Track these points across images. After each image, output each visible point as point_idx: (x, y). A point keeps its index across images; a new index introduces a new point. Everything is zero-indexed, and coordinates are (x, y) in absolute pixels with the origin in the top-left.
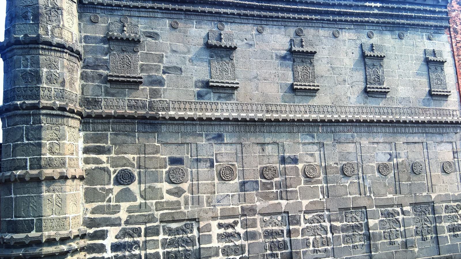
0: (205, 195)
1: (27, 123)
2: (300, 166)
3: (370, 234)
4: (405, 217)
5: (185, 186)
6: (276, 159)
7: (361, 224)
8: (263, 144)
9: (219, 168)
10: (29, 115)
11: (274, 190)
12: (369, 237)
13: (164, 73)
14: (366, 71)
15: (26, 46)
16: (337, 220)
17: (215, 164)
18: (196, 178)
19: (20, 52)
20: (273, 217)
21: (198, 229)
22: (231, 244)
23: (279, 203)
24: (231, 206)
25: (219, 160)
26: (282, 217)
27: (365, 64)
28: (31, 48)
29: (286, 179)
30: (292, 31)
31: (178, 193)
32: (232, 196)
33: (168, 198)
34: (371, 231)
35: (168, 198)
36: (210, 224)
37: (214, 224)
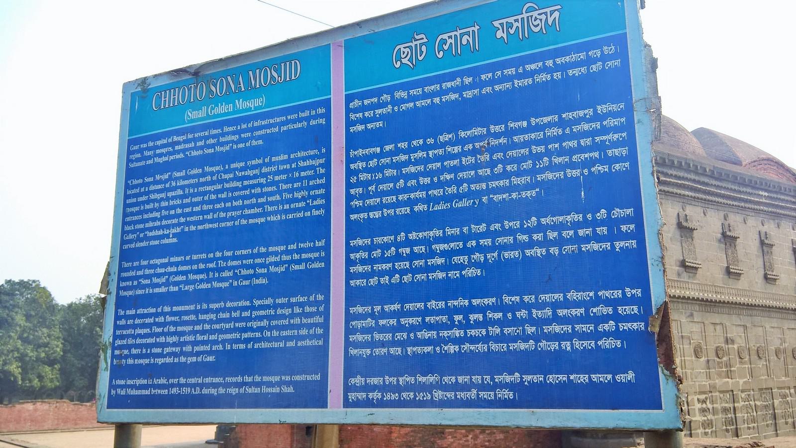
0: (689, 371)
2: (736, 346)
3: (775, 414)
4: (792, 399)
6: (722, 339)
7: (769, 404)
8: (714, 324)
9: (694, 345)
11: (724, 369)
14: (764, 258)
16: (759, 400)
17: (692, 341)
18: (728, 354)
20: (725, 394)
22: (706, 418)
23: (728, 382)
24: (704, 383)
25: (693, 338)
26: (729, 394)
27: (763, 251)
29: (730, 358)
30: (722, 214)
32: (703, 372)
34: (776, 411)
36: (693, 399)
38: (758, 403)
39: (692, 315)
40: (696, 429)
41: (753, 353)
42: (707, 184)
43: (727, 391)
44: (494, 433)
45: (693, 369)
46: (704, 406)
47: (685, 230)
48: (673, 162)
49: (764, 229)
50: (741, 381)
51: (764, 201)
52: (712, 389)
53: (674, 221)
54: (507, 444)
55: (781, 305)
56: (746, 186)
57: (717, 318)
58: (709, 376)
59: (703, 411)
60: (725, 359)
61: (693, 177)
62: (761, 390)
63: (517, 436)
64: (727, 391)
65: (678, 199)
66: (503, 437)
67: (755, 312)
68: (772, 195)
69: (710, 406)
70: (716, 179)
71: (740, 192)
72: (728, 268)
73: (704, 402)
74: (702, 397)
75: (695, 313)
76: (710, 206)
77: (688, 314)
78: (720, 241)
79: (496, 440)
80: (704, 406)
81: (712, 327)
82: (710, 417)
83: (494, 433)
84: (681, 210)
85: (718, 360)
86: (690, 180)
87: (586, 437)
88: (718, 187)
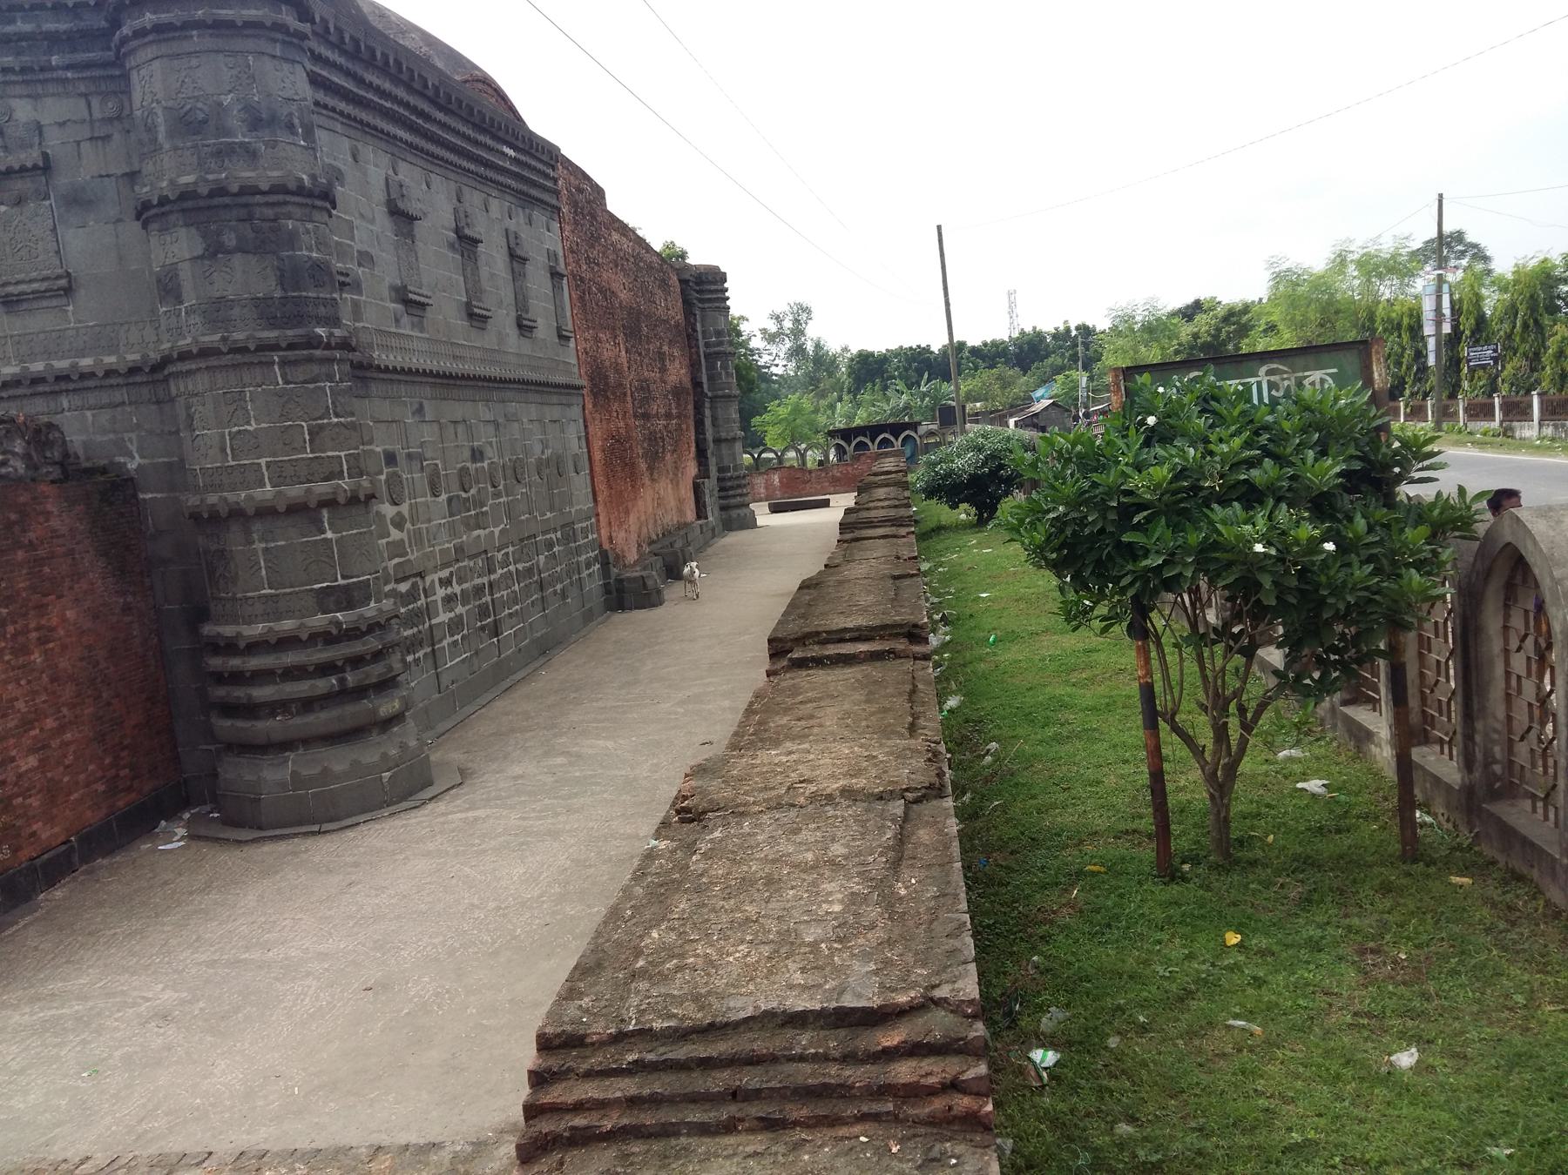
1: (330, 378)
2: (485, 465)
5: (404, 508)
6: (467, 454)
10: (331, 360)
12: (541, 586)
13: (360, 265)
15: (309, 201)
19: (297, 212)
21: (425, 590)
22: (452, 615)
28: (314, 207)
31: (399, 523)
33: (395, 534)
35: (395, 534)
37: (436, 577)
38: (520, 566)
39: (420, 410)
40: (441, 641)
41: (509, 472)
42: (427, 117)
43: (480, 554)
44: (13, 760)
45: (429, 521)
46: (449, 590)
47: (402, 218)
48: (373, 52)
49: (512, 225)
50: (497, 531)
51: (507, 165)
52: (459, 549)
53: (380, 196)
54: (49, 775)
55: (534, 376)
56: (484, 131)
57: (458, 410)
58: (453, 532)
59: (449, 600)
60: (473, 491)
61: (401, 93)
62: (522, 540)
63: (72, 748)
64: (480, 554)
65: (383, 145)
66: (35, 763)
67: (509, 394)
68: (523, 158)
69: (457, 589)
70: (441, 108)
71: (476, 143)
72: (468, 305)
73: (445, 583)
74: (445, 573)
75: (426, 403)
76: (438, 170)
77: (416, 406)
78: (451, 246)
79: (20, 776)
80: (449, 590)
81: (451, 429)
82: (460, 609)
83: (13, 760)
84: (391, 172)
85: (464, 495)
86: (401, 102)
87: (257, 718)
88: (443, 126)
